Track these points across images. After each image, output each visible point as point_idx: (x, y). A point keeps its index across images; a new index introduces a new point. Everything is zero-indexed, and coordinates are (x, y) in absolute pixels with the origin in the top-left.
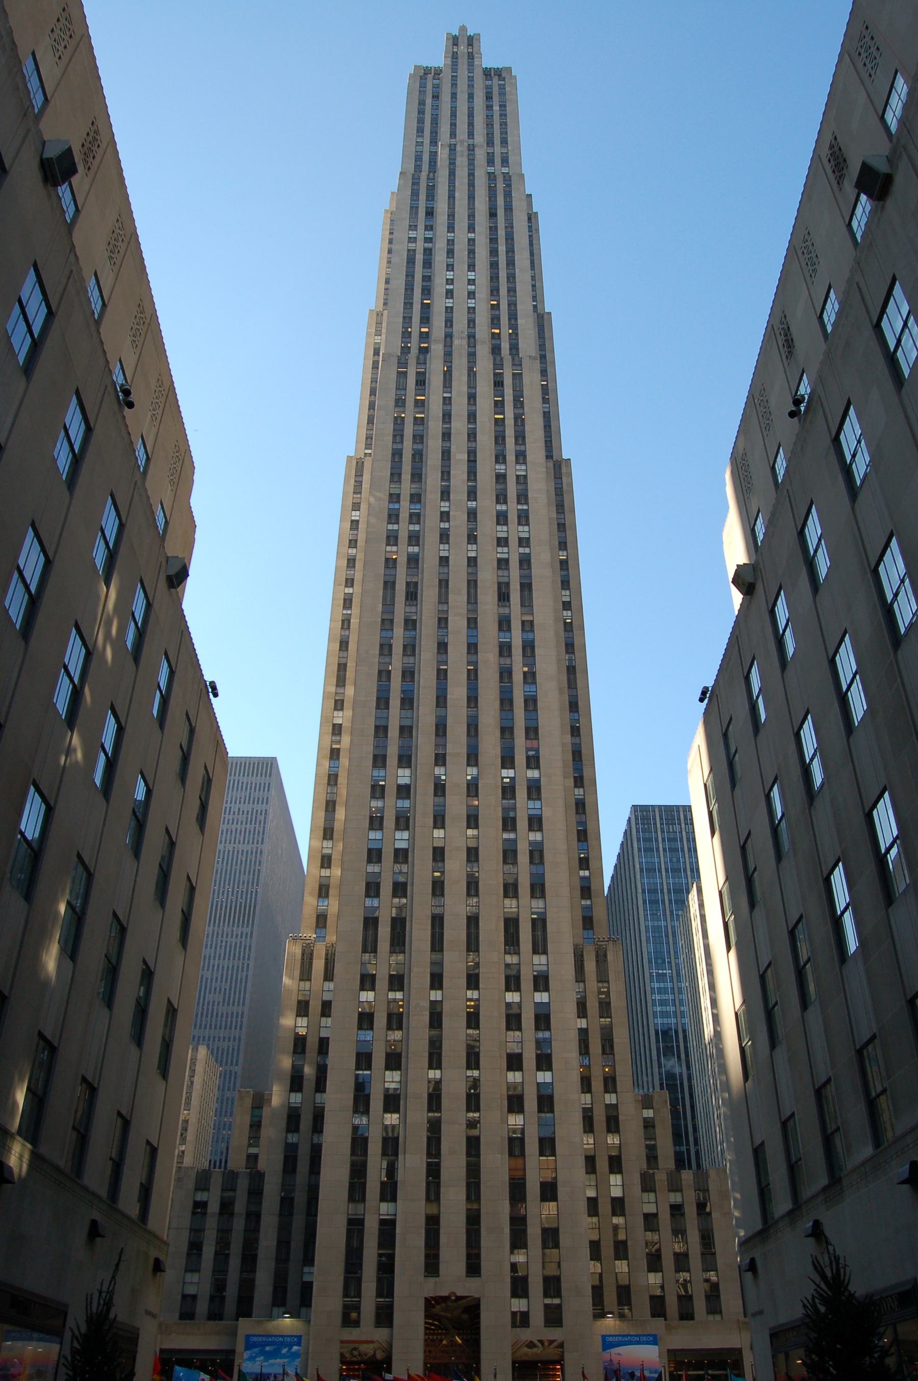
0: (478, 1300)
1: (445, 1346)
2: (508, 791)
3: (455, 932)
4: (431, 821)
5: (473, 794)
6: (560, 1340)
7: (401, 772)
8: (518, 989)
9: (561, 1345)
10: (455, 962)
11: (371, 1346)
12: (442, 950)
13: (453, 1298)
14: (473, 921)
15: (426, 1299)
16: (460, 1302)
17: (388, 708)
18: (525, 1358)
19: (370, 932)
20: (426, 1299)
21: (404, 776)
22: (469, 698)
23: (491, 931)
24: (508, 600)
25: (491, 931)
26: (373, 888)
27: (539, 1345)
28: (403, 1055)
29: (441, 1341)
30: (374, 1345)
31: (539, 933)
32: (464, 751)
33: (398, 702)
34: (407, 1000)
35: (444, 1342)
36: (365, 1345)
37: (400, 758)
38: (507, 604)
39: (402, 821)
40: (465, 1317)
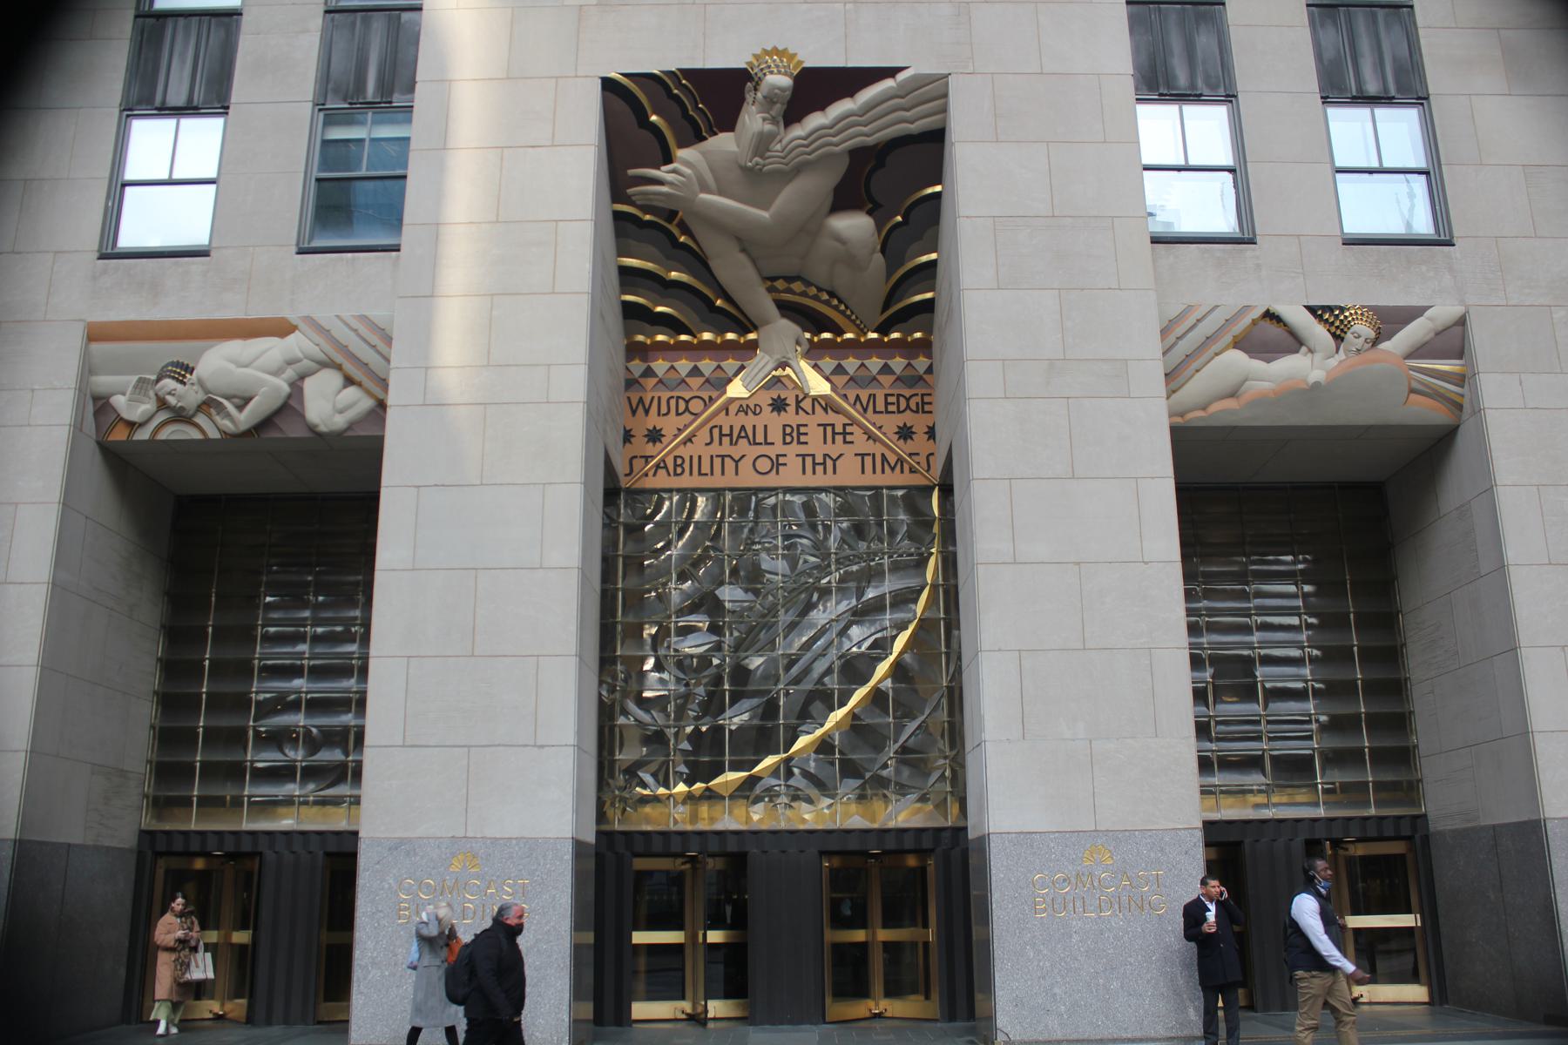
0: (934, 91)
1: (744, 408)
6: (1443, 311)
9: (1453, 340)
11: (272, 349)
13: (780, 81)
15: (608, 85)
16: (815, 120)
18: (1225, 412)
20: (608, 85)
27: (1318, 332)
29: (722, 383)
30: (296, 344)
35: (736, 389)
36: (234, 347)
40: (855, 226)
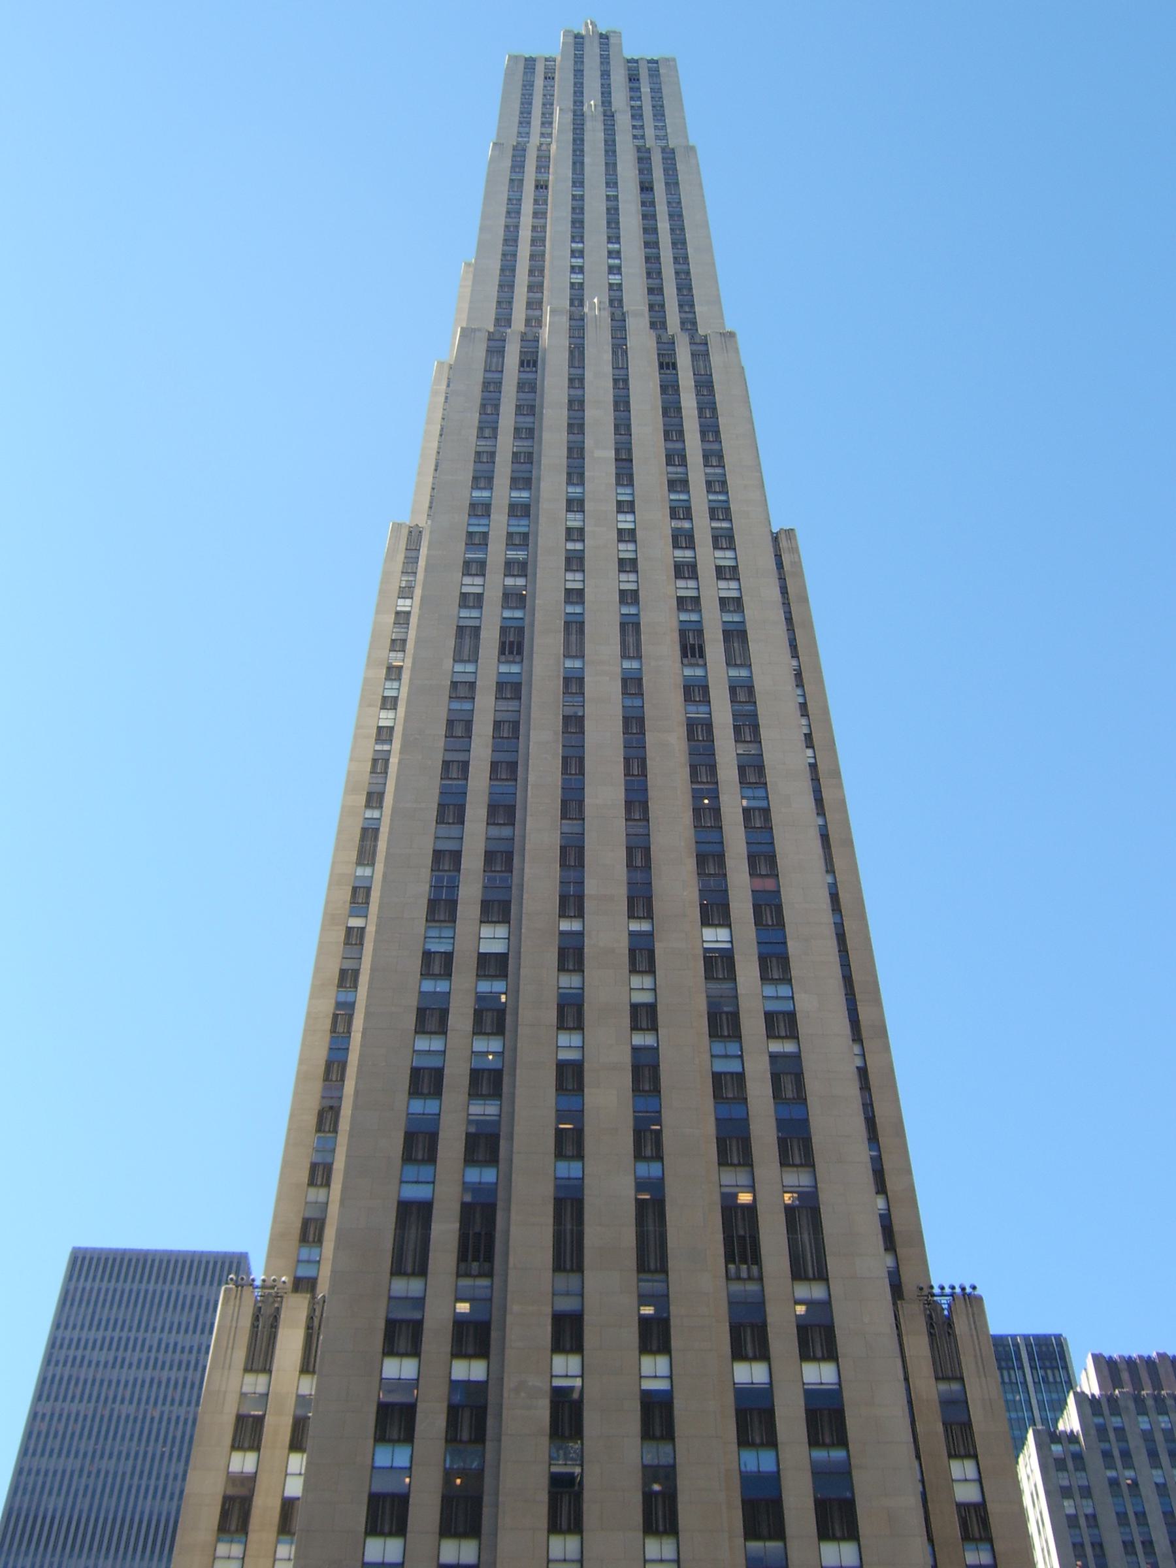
2: (719, 965)
3: (610, 1227)
4: (552, 1016)
5: (643, 966)
7: (486, 931)
8: (763, 1354)
10: (610, 1291)
12: (579, 1268)
14: (651, 1210)
17: (462, 822)
19: (413, 1233)
21: (493, 939)
22: (629, 804)
23: (694, 1229)
24: (702, 655)
25: (694, 1229)
26: (420, 1144)
28: (487, 1499)
31: (806, 1237)
32: (622, 892)
33: (483, 813)
34: (496, 1377)
37: (486, 905)
38: (701, 662)
39: (488, 1018)
